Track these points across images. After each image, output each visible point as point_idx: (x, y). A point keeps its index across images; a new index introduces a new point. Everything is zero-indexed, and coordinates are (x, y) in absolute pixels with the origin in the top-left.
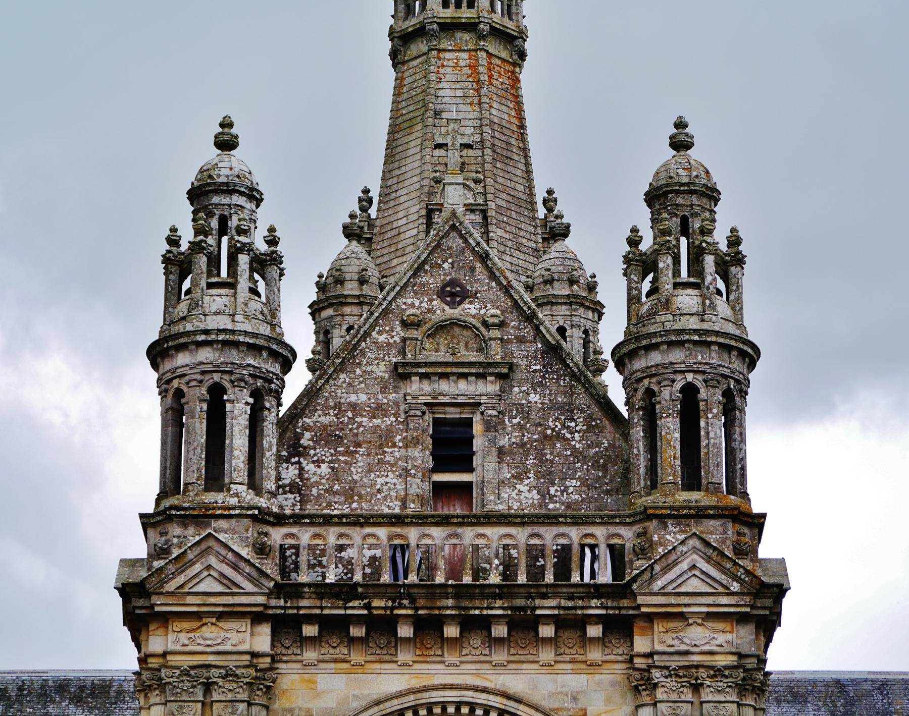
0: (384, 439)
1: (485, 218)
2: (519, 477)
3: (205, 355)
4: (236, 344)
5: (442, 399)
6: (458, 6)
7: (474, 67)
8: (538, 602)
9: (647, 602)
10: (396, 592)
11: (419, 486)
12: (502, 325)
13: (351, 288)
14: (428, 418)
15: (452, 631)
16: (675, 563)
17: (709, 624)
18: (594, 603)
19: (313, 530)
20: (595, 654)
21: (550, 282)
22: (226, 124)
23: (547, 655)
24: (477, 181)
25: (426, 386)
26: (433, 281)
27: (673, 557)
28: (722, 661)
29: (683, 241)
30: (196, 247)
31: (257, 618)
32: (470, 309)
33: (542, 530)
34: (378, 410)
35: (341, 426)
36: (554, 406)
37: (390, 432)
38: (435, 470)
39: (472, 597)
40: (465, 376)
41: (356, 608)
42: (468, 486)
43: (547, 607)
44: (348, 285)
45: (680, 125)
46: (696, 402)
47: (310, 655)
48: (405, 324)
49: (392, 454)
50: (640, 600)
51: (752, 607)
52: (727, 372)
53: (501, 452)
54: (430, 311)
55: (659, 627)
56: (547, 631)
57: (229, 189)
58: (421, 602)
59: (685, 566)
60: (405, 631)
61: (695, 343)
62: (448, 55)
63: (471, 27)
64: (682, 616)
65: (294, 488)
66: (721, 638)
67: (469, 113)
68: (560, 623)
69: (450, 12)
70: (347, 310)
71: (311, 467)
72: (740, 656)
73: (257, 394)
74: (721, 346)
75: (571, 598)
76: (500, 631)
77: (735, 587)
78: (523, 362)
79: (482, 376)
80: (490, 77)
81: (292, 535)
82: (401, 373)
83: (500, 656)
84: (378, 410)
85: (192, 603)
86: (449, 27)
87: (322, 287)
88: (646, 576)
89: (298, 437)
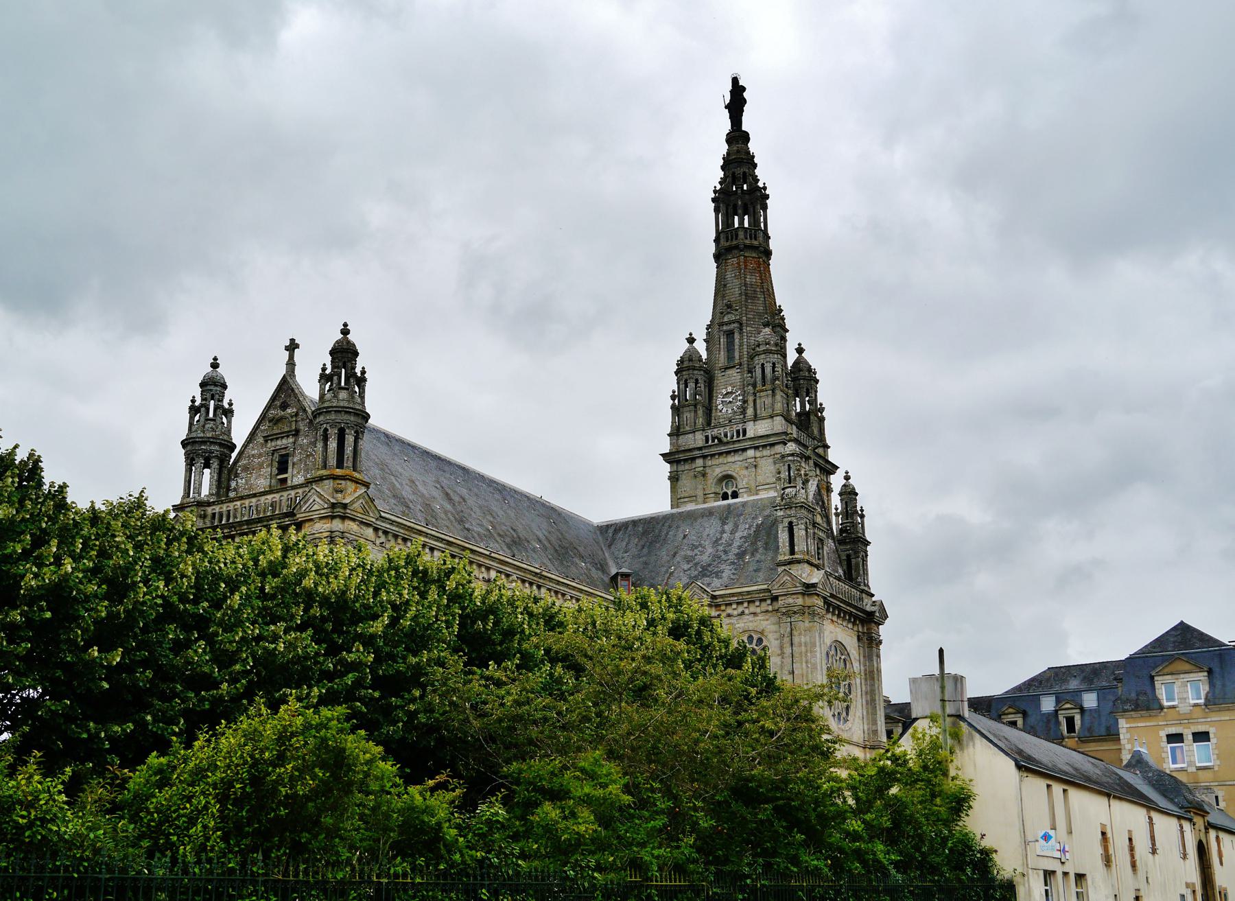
0: (261, 466)
1: (741, 324)
2: (298, 473)
4: (196, 442)
5: (278, 447)
6: (732, 240)
7: (738, 263)
8: (270, 522)
9: (300, 517)
12: (297, 415)
13: (686, 364)
14: (276, 455)
16: (308, 500)
17: (322, 521)
18: (287, 519)
19: (220, 506)
21: (759, 346)
22: (215, 359)
24: (737, 310)
25: (273, 444)
26: (278, 403)
27: (307, 498)
29: (343, 370)
30: (202, 405)
32: (289, 411)
33: (284, 493)
34: (260, 455)
35: (249, 464)
36: (311, 443)
37: (263, 462)
38: (277, 475)
39: (251, 524)
40: (282, 438)
44: (685, 363)
45: (345, 325)
46: (327, 435)
48: (270, 422)
50: (298, 516)
51: (333, 513)
52: (340, 421)
53: (294, 464)
54: (277, 414)
55: (307, 525)
58: (238, 529)
59: (311, 500)
61: (326, 412)
62: (730, 261)
63: (736, 247)
64: (311, 520)
65: (235, 490)
66: (325, 526)
67: (737, 282)
69: (728, 244)
70: (684, 373)
71: (240, 481)
72: (332, 532)
74: (335, 411)
75: (280, 519)
77: (326, 506)
78: (302, 428)
79: (288, 436)
80: (746, 266)
81: (214, 509)
82: (266, 440)
84: (260, 455)
86: (729, 250)
87: (678, 365)
88: (298, 506)
89: (237, 470)
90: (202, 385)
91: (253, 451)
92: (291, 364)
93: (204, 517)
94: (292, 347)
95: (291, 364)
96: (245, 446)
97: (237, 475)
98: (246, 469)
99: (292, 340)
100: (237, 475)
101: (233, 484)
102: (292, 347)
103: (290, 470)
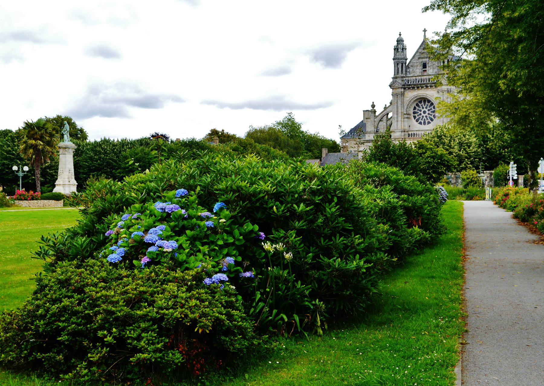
0: (417, 66)
3: (396, 60)
10: (414, 85)
11: (422, 71)
15: (420, 88)
20: (435, 89)
23: (430, 89)
26: (422, 48)
28: (446, 90)
31: (402, 88)
41: (410, 87)
42: (426, 70)
43: (428, 85)
47: (408, 91)
49: (418, 67)
56: (429, 87)
57: (399, 41)
60: (416, 88)
68: (431, 86)
73: (402, 64)
76: (425, 88)
82: (419, 58)
83: (426, 90)
84: (417, 63)
85: (395, 87)
90: (397, 41)
91: (413, 61)
92: (425, 36)
93: (403, 81)
94: (425, 31)
95: (425, 36)
96: (411, 59)
97: (409, 68)
98: (412, 66)
99: (425, 29)
100: (409, 68)
101: (408, 70)
102: (425, 31)
103: (427, 69)
